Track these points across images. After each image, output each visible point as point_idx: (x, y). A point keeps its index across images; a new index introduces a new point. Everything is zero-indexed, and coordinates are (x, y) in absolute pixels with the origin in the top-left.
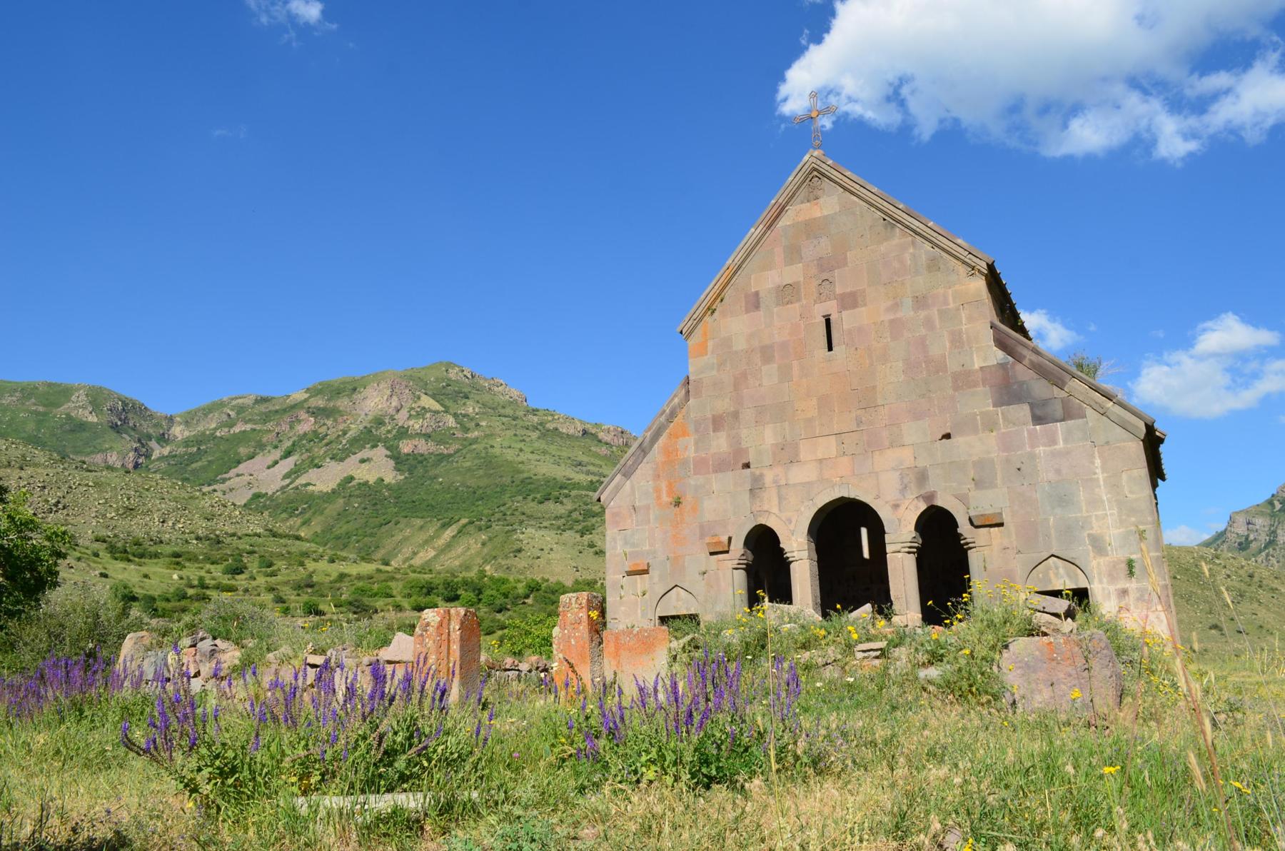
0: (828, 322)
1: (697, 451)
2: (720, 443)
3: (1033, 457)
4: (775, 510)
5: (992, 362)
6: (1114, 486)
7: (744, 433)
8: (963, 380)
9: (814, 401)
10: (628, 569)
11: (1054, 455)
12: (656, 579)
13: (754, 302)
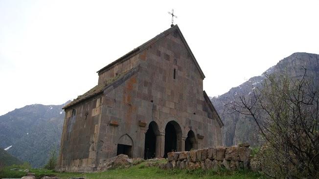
0: (175, 70)
1: (139, 89)
2: (145, 91)
3: (207, 125)
4: (158, 118)
5: (203, 100)
6: (217, 136)
7: (153, 91)
8: (198, 101)
9: (170, 91)
10: (111, 123)
11: (210, 126)
12: (120, 130)
13: (159, 54)
